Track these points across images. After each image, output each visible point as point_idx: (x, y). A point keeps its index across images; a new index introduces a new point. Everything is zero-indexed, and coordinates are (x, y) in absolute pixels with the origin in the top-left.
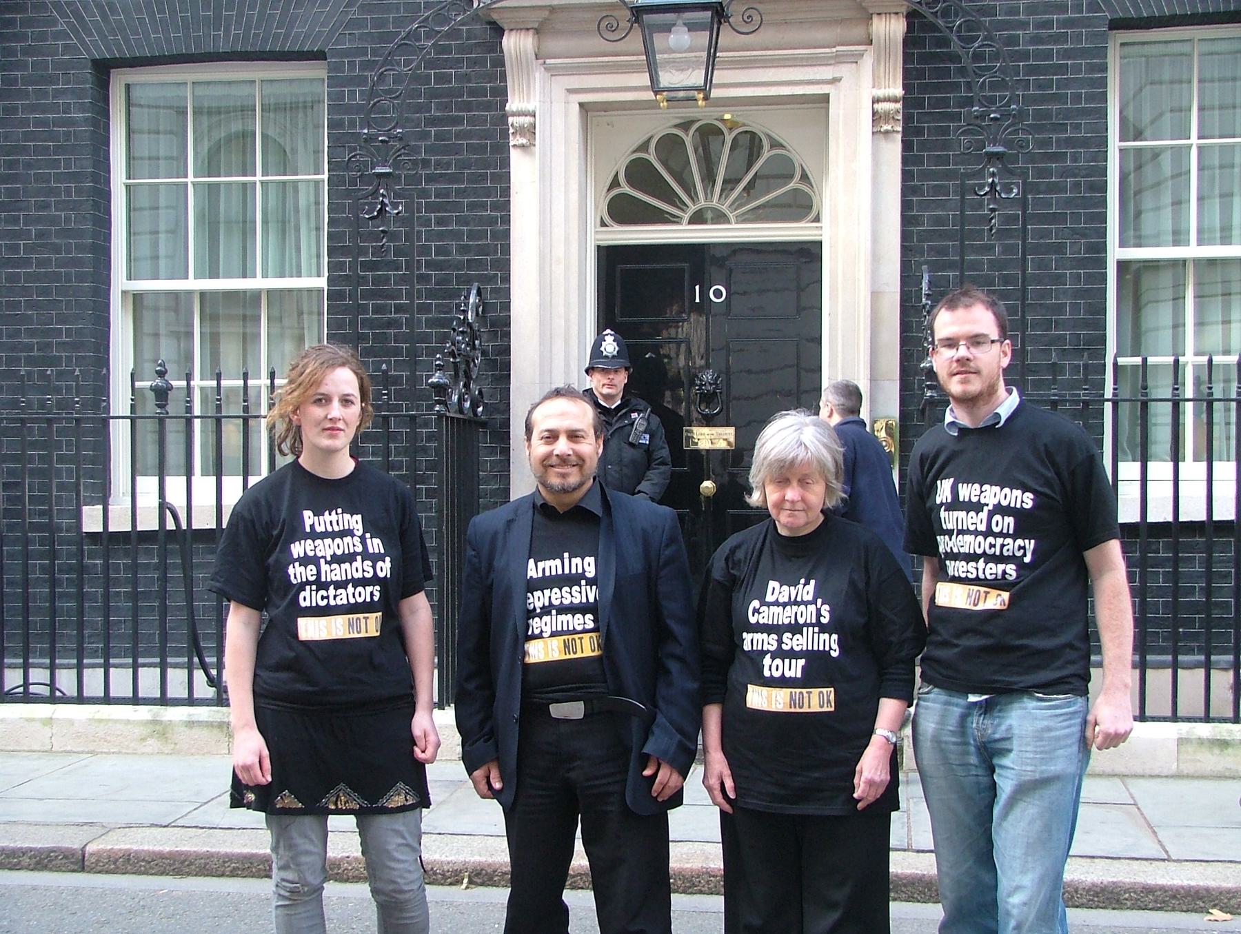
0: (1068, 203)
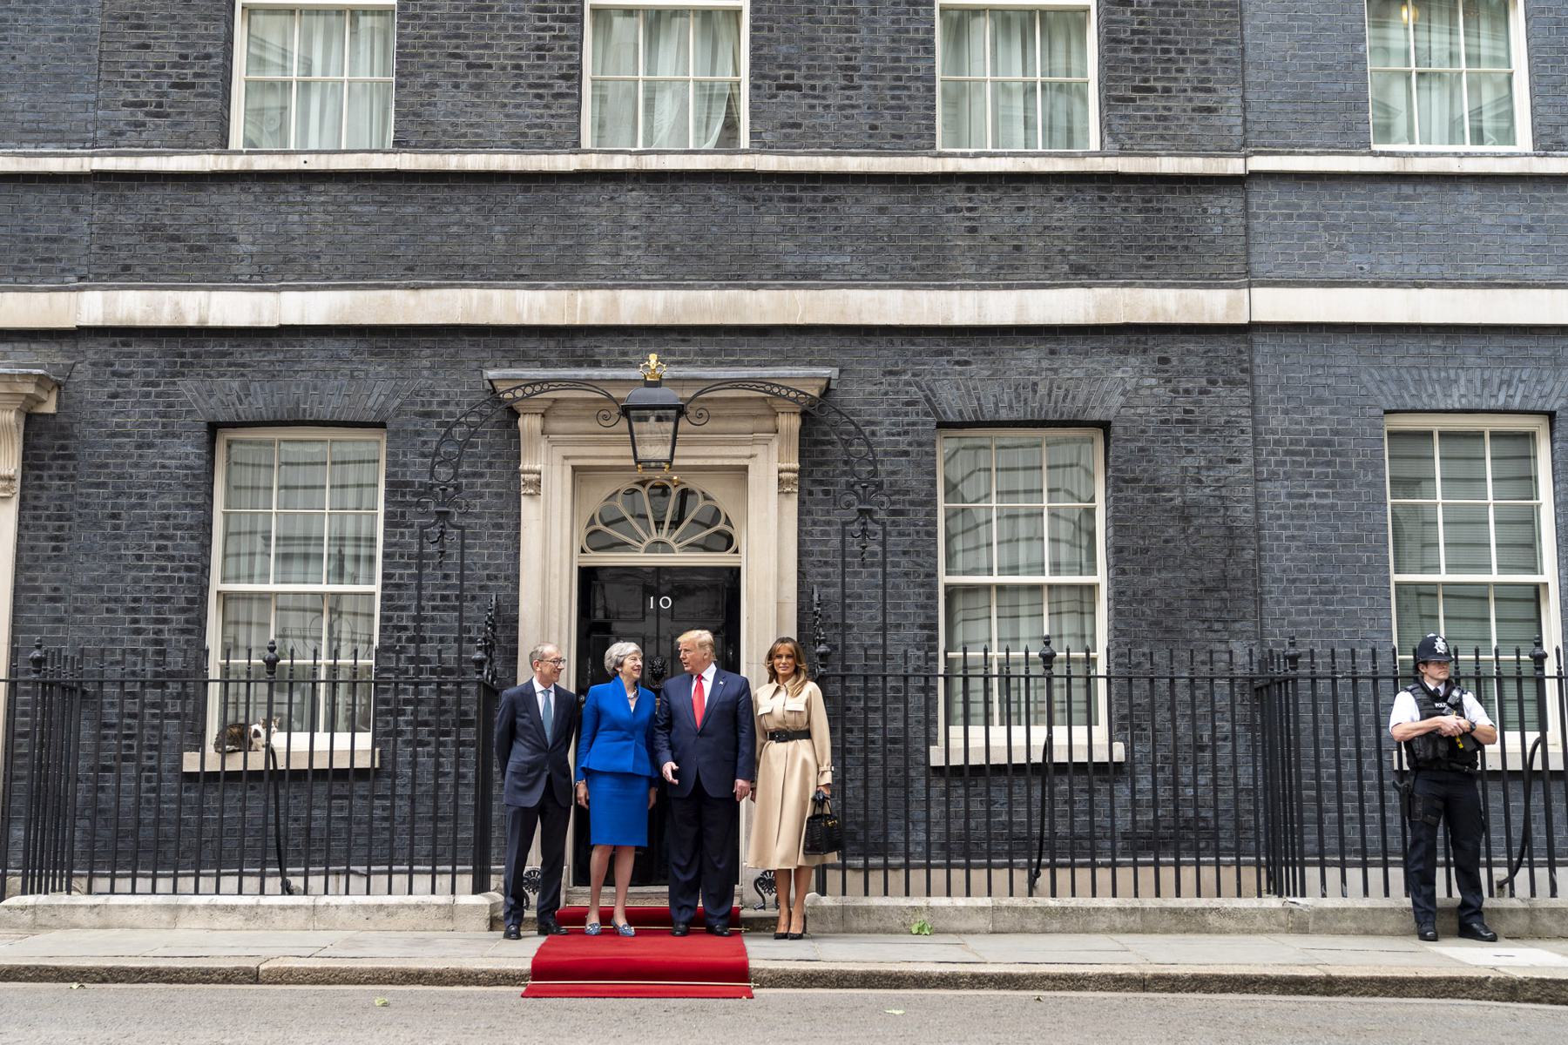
0: (912, 544)
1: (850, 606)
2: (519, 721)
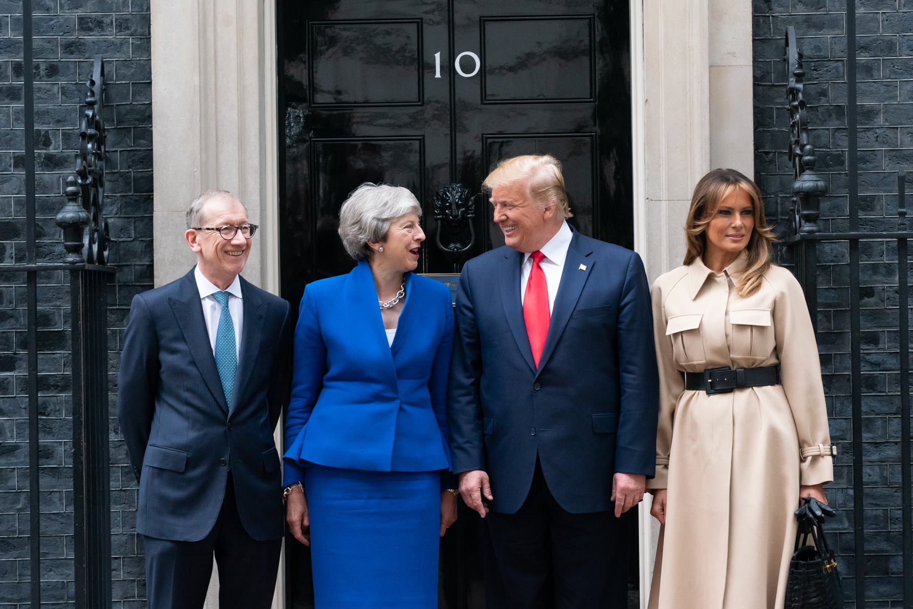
1: (868, 69)
2: (166, 358)
